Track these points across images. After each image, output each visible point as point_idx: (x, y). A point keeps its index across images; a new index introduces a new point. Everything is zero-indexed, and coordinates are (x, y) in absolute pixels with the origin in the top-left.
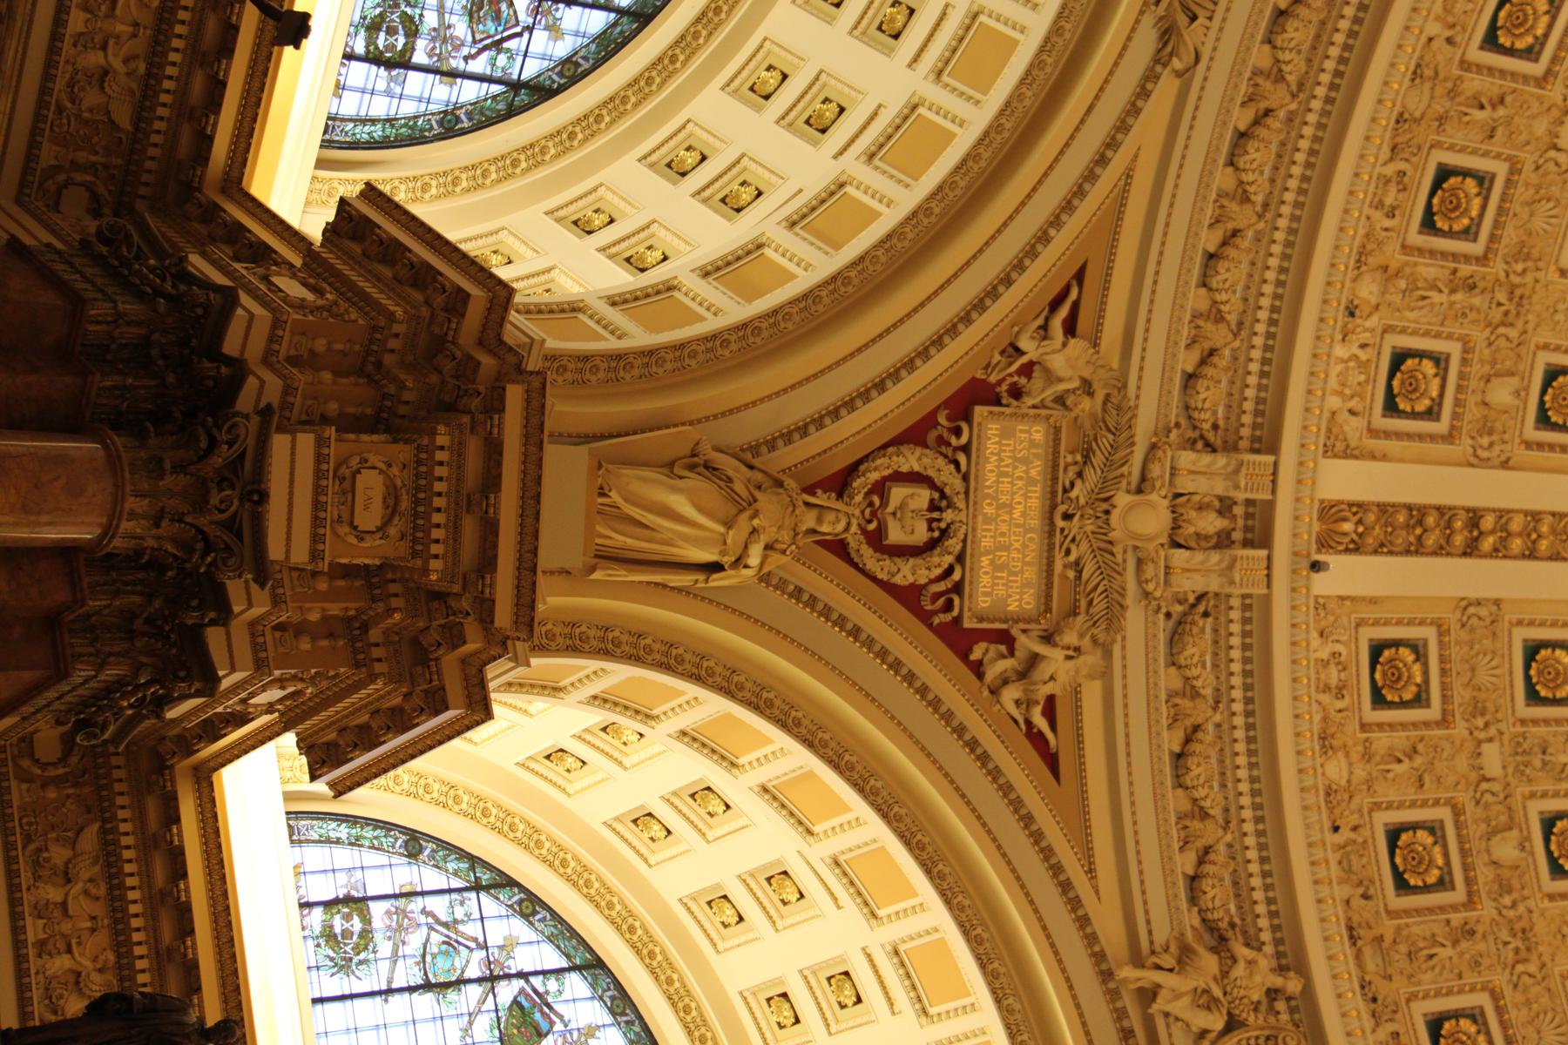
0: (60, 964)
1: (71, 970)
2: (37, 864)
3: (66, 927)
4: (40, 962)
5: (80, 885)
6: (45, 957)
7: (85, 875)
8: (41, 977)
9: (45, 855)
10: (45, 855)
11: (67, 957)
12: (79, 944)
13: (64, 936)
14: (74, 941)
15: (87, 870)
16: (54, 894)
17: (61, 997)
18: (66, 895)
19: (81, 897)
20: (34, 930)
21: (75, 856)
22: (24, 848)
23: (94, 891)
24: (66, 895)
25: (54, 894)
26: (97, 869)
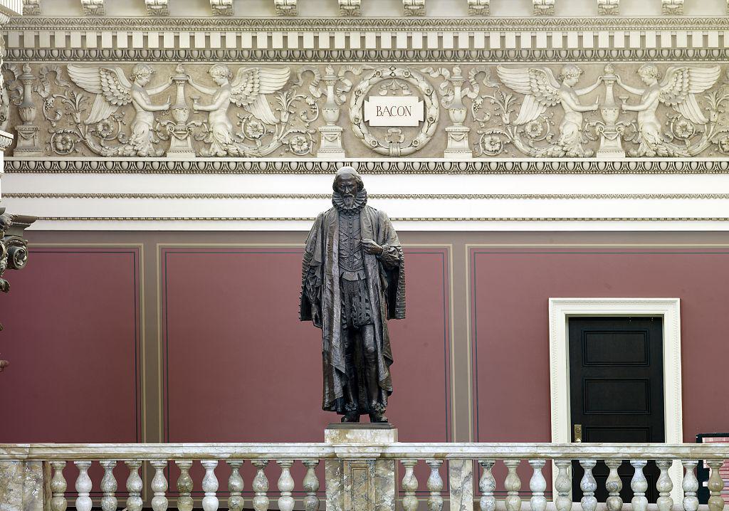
0: (221, 126)
1: (228, 113)
2: (540, 140)
3: (182, 116)
4: (216, 148)
5: (137, 95)
6: (210, 139)
8: (662, 150)
9: (528, 128)
10: (100, 128)
11: (212, 117)
12: (200, 101)
13: (190, 119)
14: (197, 107)
15: (119, 82)
16: (145, 123)
18: (147, 111)
19: (149, 92)
21: (532, 94)
22: (521, 154)
23: (145, 80)
24: (147, 111)
25: (145, 123)
26: (120, 72)
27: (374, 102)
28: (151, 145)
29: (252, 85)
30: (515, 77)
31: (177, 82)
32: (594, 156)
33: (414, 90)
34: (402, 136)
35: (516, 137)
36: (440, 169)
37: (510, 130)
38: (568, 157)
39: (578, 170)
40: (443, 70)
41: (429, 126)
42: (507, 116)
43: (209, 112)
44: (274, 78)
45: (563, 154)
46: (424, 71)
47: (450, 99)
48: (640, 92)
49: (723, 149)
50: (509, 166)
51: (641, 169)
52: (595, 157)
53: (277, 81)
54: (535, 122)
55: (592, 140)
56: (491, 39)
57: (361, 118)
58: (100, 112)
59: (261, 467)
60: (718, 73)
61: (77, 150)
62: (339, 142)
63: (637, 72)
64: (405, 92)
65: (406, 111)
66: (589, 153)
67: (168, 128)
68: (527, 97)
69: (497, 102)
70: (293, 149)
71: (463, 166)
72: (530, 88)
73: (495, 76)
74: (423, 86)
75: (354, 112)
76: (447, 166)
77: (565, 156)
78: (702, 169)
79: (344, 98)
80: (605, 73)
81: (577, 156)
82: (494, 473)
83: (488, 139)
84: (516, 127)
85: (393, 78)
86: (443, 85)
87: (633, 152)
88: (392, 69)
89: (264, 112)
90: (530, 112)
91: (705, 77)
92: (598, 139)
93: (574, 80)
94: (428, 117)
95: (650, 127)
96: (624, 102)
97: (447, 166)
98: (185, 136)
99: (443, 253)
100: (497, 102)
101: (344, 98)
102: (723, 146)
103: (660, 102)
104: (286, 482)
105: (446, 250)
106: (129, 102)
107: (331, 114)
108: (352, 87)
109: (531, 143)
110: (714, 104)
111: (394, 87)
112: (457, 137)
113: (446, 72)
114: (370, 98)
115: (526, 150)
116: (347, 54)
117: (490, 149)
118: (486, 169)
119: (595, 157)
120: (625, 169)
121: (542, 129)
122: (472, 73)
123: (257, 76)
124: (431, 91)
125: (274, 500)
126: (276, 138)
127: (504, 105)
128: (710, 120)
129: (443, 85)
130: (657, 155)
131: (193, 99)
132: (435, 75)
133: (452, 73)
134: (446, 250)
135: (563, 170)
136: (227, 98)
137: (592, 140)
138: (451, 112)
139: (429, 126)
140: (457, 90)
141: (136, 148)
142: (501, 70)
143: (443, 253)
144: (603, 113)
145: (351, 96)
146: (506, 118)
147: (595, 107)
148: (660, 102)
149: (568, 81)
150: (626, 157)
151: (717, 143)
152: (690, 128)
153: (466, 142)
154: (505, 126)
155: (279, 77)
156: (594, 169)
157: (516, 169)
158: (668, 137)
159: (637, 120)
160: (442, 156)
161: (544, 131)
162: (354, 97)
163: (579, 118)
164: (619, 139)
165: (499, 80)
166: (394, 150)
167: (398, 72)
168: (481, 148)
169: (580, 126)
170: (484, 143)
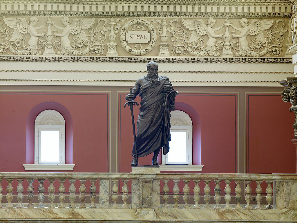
2: (20, 48)
3: (49, 39)
7: (26, 26)
9: (15, 42)
17: (80, 44)
20: (49, 53)
27: (130, 33)
28: (37, 50)
29: (79, 26)
30: (188, 23)
31: (48, 24)
32: (42, 54)
33: (147, 28)
34: (141, 47)
35: (11, 46)
36: (104, 60)
37: (8, 43)
38: (31, 55)
39: (34, 60)
40: (159, 20)
41: (152, 43)
42: (7, 38)
43: (60, 37)
44: (88, 22)
45: (29, 53)
46: (151, 21)
47: (161, 32)
48: (62, 28)
49: (95, 52)
50: (89, 59)
51: (60, 60)
52: (43, 55)
53: (89, 24)
54: (18, 40)
55: (41, 48)
56: (67, 7)
57: (124, 39)
58: (15, 37)
59: (83, 183)
60: (273, 23)
61: (6, 52)
62: (115, 49)
63: (61, 21)
64: (144, 29)
65: (141, 37)
66: (40, 52)
67: (44, 43)
68: (15, 30)
69: (3, 32)
70: (95, 52)
71: (114, 59)
72: (16, 26)
73: (180, 23)
74: (150, 27)
75: (123, 37)
76: (108, 59)
77: (30, 54)
78: (86, 60)
79: (117, 32)
80: (48, 21)
81: (35, 55)
82: (189, 186)
83: (177, 48)
84: (188, 44)
85: (138, 23)
86: (158, 27)
87: (236, 54)
88: (138, 19)
89: (84, 38)
90: (15, 37)
91: (268, 24)
92: (44, 48)
93: (35, 23)
94: (152, 39)
95: (66, 42)
96: (55, 32)
97: (108, 59)
98: (51, 47)
99: (107, 95)
100: (3, 32)
101: (117, 32)
102: (274, 52)
103: (70, 33)
104: (20, 187)
105: (109, 93)
106: (28, 32)
107: (113, 39)
108: (121, 27)
109: (16, 48)
110: (92, 34)
111: (138, 27)
112: (165, 48)
113: (160, 22)
114: (128, 31)
115: (14, 51)
116: (110, 14)
117: (178, 53)
118: (174, 61)
119: (43, 55)
120: (54, 60)
121: (199, 44)
122: (172, 21)
123: (81, 22)
124: (154, 28)
125: (68, 195)
126: (88, 48)
127: (5, 33)
128: (268, 41)
129: (158, 27)
130: (68, 55)
131: (54, 32)
132: (155, 22)
133: (162, 22)
134: (109, 93)
135: (28, 60)
136: (69, 31)
137: (41, 48)
138: (162, 38)
139: (152, 43)
140: (164, 28)
141: (30, 51)
142: (183, 20)
143: (107, 95)
144: (46, 37)
145: (120, 31)
146: (6, 39)
147: (43, 34)
148: (70, 33)
149: (33, 24)
150: (233, 56)
151: (93, 50)
152: (82, 43)
153: (168, 50)
154: (184, 43)
155: (90, 23)
156: (41, 60)
157: (187, 61)
158: (73, 47)
159: (60, 40)
160: (106, 55)
161: (22, 45)
162: (122, 31)
163: (37, 38)
164: (52, 48)
165: (4, 23)
166: (138, 52)
167: (140, 21)
168: (174, 53)
169: (37, 42)
170: (175, 50)
